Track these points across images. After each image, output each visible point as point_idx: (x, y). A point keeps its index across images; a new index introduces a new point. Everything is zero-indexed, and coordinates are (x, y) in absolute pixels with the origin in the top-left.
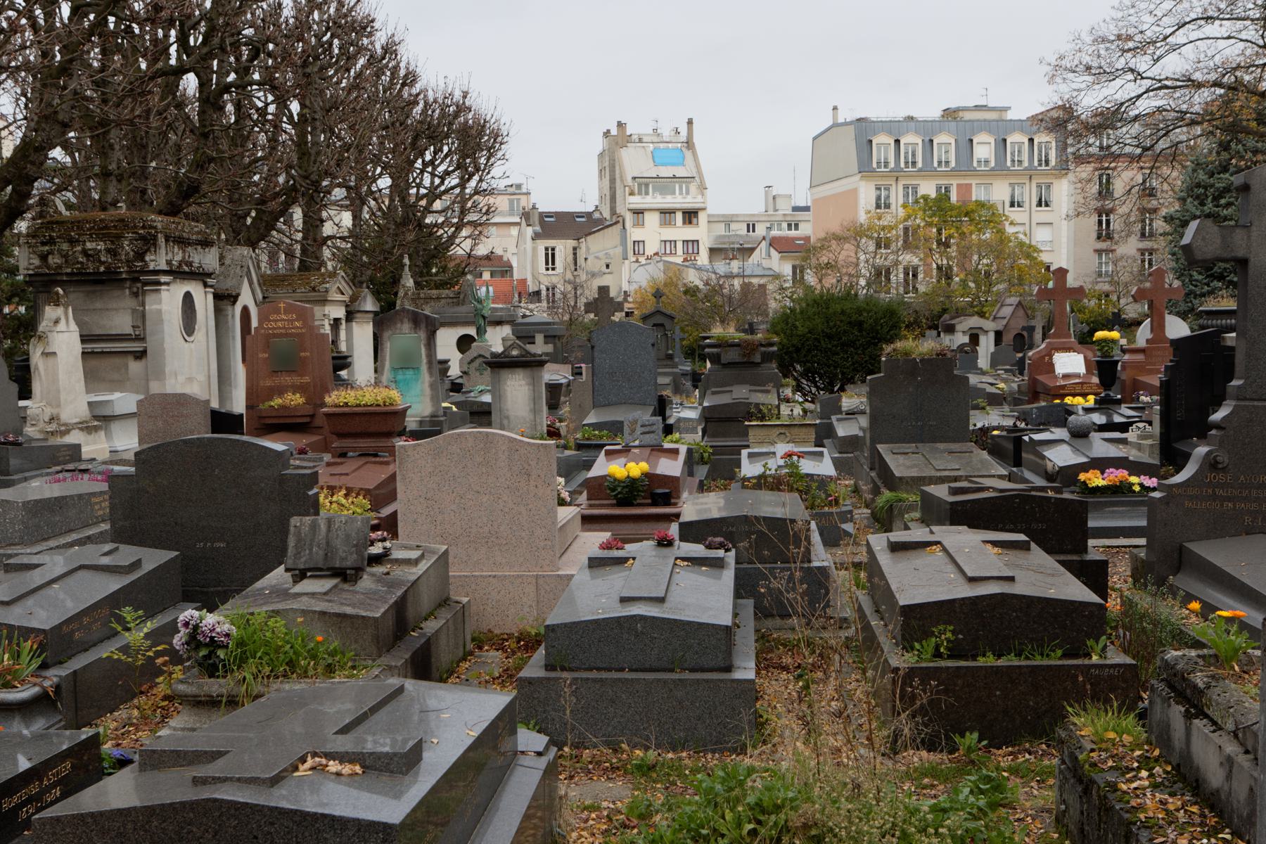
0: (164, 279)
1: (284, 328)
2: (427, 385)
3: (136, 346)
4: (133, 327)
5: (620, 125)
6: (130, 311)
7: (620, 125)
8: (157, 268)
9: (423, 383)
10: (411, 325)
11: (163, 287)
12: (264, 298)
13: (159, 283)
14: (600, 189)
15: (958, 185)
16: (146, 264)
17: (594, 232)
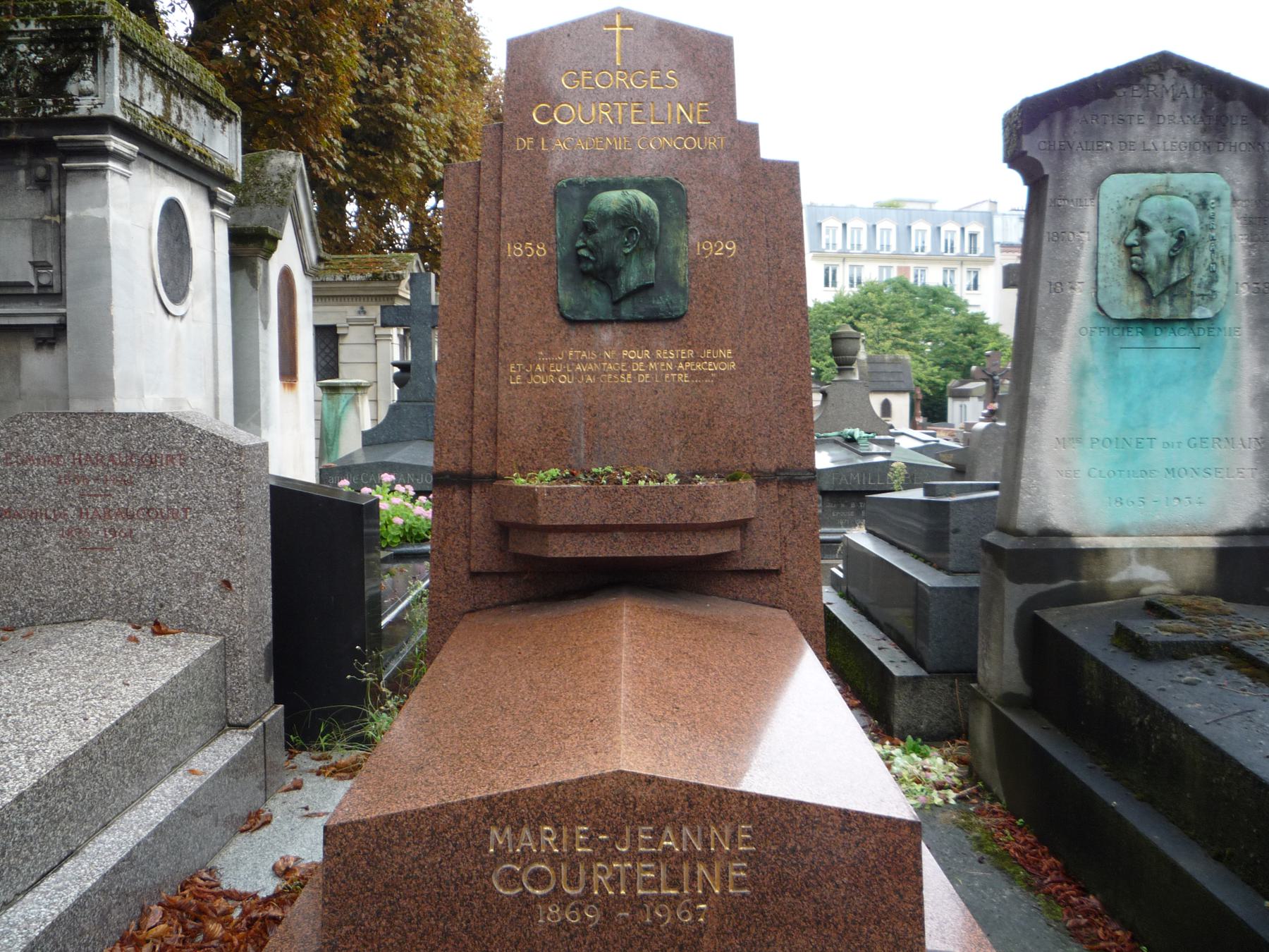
0: (116, 143)
2: (1246, 393)
3: (37, 314)
4: (35, 264)
6: (27, 225)
8: (98, 112)
9: (1230, 385)
10: (1189, 132)
11: (111, 164)
13: (106, 154)
16: (70, 103)
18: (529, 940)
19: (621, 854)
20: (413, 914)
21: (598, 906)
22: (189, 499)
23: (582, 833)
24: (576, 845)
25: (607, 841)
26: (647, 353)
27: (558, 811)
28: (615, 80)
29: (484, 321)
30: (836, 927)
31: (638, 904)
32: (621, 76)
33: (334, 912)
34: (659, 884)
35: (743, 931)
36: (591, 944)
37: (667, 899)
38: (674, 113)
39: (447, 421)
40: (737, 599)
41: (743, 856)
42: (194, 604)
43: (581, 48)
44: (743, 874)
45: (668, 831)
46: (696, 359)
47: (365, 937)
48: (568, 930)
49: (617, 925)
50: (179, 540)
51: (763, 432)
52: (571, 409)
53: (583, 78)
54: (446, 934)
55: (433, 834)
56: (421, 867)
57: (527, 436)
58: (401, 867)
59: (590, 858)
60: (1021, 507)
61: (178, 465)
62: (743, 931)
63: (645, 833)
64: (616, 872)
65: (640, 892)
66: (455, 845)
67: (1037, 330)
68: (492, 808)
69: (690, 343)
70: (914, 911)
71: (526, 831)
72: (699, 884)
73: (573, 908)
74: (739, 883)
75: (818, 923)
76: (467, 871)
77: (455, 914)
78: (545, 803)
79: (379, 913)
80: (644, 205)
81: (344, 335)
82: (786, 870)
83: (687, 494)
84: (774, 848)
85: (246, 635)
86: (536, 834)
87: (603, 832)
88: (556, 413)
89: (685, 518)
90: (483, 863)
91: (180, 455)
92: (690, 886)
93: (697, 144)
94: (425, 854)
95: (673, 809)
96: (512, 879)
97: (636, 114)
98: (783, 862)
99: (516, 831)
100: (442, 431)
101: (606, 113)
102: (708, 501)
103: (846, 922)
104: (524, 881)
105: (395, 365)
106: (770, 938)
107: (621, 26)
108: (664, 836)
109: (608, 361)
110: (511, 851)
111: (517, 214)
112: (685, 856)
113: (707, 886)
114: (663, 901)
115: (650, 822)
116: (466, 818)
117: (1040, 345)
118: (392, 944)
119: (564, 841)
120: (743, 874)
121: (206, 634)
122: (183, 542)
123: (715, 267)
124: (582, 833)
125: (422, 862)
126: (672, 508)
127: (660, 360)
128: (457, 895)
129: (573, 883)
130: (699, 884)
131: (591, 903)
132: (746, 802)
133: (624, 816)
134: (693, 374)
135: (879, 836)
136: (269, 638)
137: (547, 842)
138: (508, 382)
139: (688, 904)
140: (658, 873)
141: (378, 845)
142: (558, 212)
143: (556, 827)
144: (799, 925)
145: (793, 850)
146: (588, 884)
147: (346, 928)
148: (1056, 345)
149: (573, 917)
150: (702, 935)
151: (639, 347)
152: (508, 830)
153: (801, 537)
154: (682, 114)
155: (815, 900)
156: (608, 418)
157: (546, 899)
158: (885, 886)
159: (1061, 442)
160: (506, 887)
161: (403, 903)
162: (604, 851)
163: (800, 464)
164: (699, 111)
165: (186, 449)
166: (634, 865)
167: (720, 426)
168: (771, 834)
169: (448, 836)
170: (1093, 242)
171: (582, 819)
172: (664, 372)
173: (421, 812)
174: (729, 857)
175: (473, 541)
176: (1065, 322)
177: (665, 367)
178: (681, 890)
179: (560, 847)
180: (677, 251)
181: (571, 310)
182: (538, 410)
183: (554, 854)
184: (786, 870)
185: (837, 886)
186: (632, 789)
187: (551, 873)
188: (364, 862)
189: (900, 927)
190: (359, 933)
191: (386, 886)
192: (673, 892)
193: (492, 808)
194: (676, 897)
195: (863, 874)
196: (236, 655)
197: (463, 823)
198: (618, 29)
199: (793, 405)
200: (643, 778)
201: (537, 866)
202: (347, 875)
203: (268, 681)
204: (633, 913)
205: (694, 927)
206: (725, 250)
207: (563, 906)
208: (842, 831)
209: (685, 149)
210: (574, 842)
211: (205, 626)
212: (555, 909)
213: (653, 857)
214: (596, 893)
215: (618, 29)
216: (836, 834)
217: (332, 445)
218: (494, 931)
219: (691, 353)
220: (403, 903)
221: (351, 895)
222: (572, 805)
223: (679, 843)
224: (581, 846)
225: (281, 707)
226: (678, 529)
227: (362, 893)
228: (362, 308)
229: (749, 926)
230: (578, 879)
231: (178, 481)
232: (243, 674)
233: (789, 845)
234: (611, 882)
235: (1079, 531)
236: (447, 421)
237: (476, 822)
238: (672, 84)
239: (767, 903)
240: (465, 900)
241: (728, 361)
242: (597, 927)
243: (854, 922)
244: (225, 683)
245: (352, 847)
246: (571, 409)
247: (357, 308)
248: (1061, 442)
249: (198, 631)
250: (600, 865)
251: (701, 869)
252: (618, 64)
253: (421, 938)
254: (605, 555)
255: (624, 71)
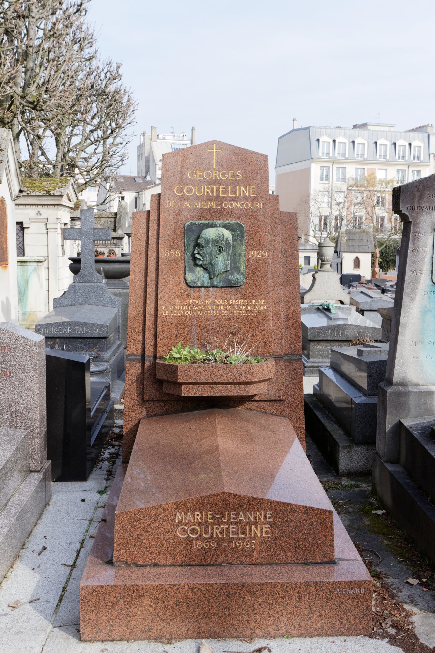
1: (217, 198)
5: (153, 128)
7: (153, 128)
12: (21, 191)
14: (138, 167)
15: (368, 169)
17: (149, 188)
18: (190, 554)
19: (224, 522)
20: (148, 545)
21: (215, 541)
22: (12, 367)
23: (210, 515)
24: (208, 519)
25: (219, 518)
26: (226, 302)
27: (201, 507)
28: (213, 175)
29: (151, 285)
30: (302, 549)
31: (231, 540)
32: (216, 173)
33: (118, 545)
34: (238, 533)
35: (268, 550)
36: (213, 555)
37: (241, 539)
38: (240, 191)
39: (133, 331)
40: (265, 413)
41: (269, 523)
42: (14, 415)
43: (197, 160)
44: (268, 529)
45: (241, 514)
46: (248, 304)
47: (130, 554)
48: (205, 550)
49: (222, 548)
50: (7, 386)
51: (278, 337)
52: (191, 327)
53: (198, 174)
54: (160, 552)
55: (155, 516)
56: (151, 528)
57: (170, 339)
58: (143, 528)
59: (213, 524)
60: (395, 372)
61: (7, 351)
62: (268, 550)
63: (233, 515)
64: (222, 529)
65: (231, 536)
66: (163, 520)
67: (404, 292)
68: (177, 506)
69: (245, 297)
70: (331, 543)
71: (189, 514)
72: (253, 533)
73: (206, 542)
74: (267, 533)
75: (296, 547)
76: (168, 529)
77: (163, 545)
78: (197, 504)
79: (135, 545)
80: (226, 236)
81: (28, 228)
82: (284, 528)
83: (244, 369)
84: (280, 520)
85: (39, 430)
86: (193, 515)
87: (218, 514)
88: (184, 328)
89: (243, 379)
90: (174, 526)
91: (8, 347)
92: (249, 534)
93: (250, 205)
94: (153, 523)
95: (243, 506)
96: (185, 531)
97: (222, 191)
98: (283, 525)
99: (186, 514)
100: (130, 335)
101: (209, 191)
102: (253, 372)
103: (306, 547)
104: (189, 532)
105: (70, 259)
106: (278, 553)
107: (216, 150)
108: (240, 516)
109: (208, 305)
110: (184, 521)
111: (167, 237)
112: (248, 523)
113: (255, 534)
114: (239, 540)
115: (235, 511)
116: (168, 510)
117: (405, 299)
118: (139, 557)
119: (204, 518)
120: (268, 529)
121: (20, 429)
122: (9, 387)
123: (258, 263)
124: (210, 515)
125: (151, 526)
126: (237, 375)
127: (231, 305)
128: (164, 538)
129: (207, 533)
130: (253, 533)
131: (213, 540)
132: (270, 504)
133: (225, 508)
134: (247, 311)
135: (318, 516)
136: (46, 429)
137: (197, 518)
138: (162, 314)
139: (248, 541)
140: (238, 529)
141: (135, 520)
142: (186, 237)
143: (201, 513)
144: (289, 548)
145: (287, 521)
146: (212, 533)
147: (122, 551)
148: (413, 299)
149: (206, 545)
150: (253, 552)
151: (222, 299)
152: (183, 514)
153: (295, 385)
154: (243, 191)
155: (295, 539)
156: (208, 331)
157: (197, 539)
158: (320, 534)
159: (414, 343)
160: (182, 535)
161: (144, 541)
162: (218, 522)
163: (295, 352)
164: (251, 190)
165: (11, 344)
166: (229, 526)
167: (258, 335)
168: (279, 515)
169: (161, 516)
170: (431, 252)
171: (210, 509)
172: (234, 310)
173: (151, 508)
174: (264, 523)
175: (145, 386)
176: (417, 289)
177: (234, 308)
178: (246, 536)
179: (202, 520)
180: (240, 255)
181: (190, 283)
182: (176, 327)
183: (200, 523)
184: (284, 528)
185: (303, 534)
186: (228, 499)
187: (199, 529)
188: (130, 526)
189: (325, 549)
190: (127, 553)
191: (138, 535)
192: (243, 536)
193: (177, 506)
194: (244, 538)
195: (312, 529)
196: (34, 439)
197: (167, 512)
198: (214, 151)
199: (292, 325)
200: (232, 495)
201: (193, 527)
202: (123, 531)
203: (45, 450)
204: (228, 544)
205: (251, 549)
206: (262, 254)
207: (203, 542)
208: (305, 514)
209: (245, 208)
210: (207, 518)
211: (19, 425)
212: (200, 542)
213: (236, 523)
214: (215, 536)
215: (214, 151)
216: (302, 515)
217: (23, 296)
218: (178, 551)
219: (246, 302)
220: (144, 541)
221: (124, 538)
222: (207, 505)
223: (245, 518)
224: (210, 519)
225: (50, 461)
226: (239, 383)
227: (129, 538)
228: (39, 212)
229: (270, 549)
230: (208, 532)
231: (7, 358)
232: (37, 447)
233: (285, 519)
234: (221, 533)
235: (421, 384)
236: (133, 331)
237: (171, 511)
238: (239, 177)
239: (277, 540)
240: (167, 540)
241: (263, 305)
242: (215, 549)
243: (308, 547)
244: (29, 452)
245: (125, 521)
246: (191, 327)
247: (36, 212)
248: (414, 343)
249: (16, 427)
250: (216, 526)
251: (253, 527)
252: (214, 167)
253: (150, 554)
254: (207, 395)
255: (217, 171)
